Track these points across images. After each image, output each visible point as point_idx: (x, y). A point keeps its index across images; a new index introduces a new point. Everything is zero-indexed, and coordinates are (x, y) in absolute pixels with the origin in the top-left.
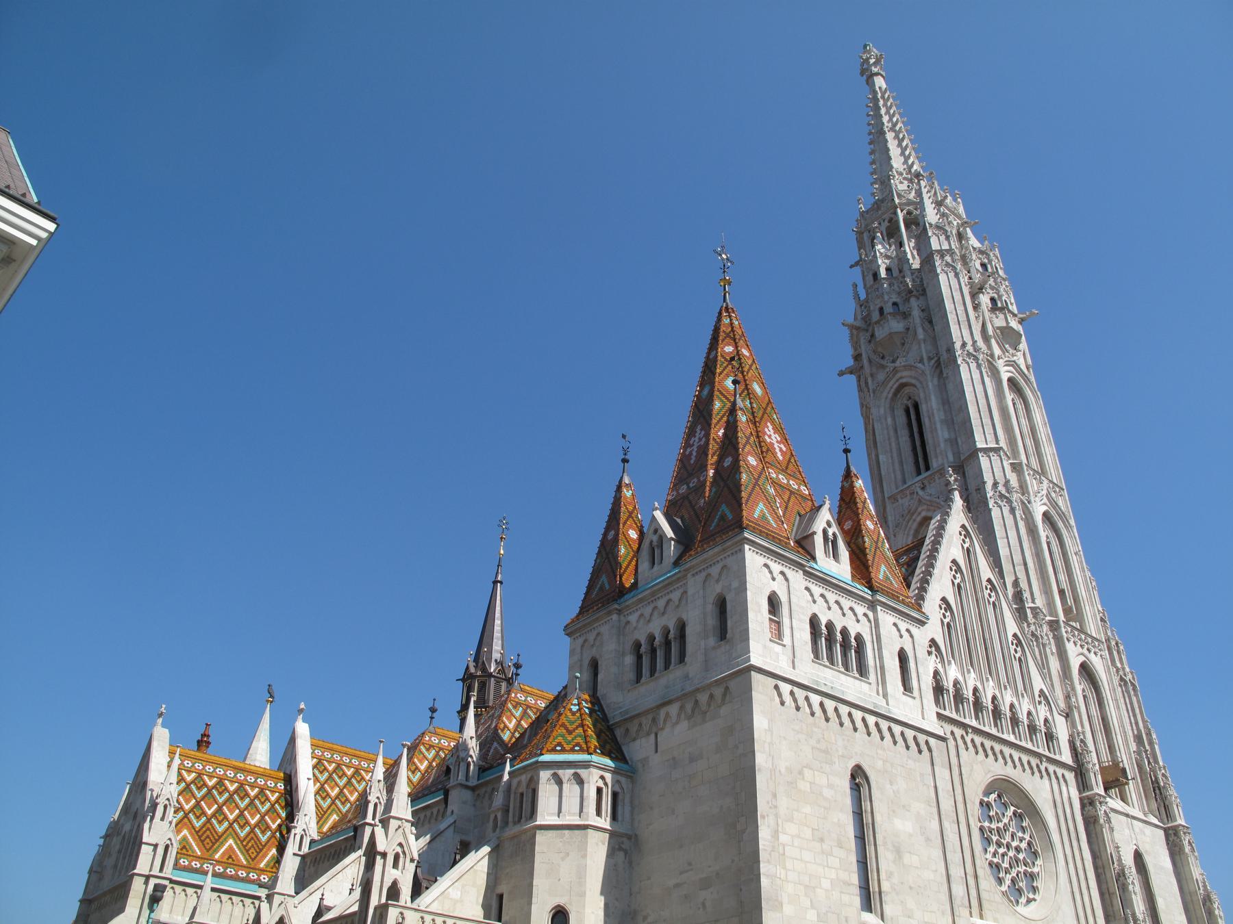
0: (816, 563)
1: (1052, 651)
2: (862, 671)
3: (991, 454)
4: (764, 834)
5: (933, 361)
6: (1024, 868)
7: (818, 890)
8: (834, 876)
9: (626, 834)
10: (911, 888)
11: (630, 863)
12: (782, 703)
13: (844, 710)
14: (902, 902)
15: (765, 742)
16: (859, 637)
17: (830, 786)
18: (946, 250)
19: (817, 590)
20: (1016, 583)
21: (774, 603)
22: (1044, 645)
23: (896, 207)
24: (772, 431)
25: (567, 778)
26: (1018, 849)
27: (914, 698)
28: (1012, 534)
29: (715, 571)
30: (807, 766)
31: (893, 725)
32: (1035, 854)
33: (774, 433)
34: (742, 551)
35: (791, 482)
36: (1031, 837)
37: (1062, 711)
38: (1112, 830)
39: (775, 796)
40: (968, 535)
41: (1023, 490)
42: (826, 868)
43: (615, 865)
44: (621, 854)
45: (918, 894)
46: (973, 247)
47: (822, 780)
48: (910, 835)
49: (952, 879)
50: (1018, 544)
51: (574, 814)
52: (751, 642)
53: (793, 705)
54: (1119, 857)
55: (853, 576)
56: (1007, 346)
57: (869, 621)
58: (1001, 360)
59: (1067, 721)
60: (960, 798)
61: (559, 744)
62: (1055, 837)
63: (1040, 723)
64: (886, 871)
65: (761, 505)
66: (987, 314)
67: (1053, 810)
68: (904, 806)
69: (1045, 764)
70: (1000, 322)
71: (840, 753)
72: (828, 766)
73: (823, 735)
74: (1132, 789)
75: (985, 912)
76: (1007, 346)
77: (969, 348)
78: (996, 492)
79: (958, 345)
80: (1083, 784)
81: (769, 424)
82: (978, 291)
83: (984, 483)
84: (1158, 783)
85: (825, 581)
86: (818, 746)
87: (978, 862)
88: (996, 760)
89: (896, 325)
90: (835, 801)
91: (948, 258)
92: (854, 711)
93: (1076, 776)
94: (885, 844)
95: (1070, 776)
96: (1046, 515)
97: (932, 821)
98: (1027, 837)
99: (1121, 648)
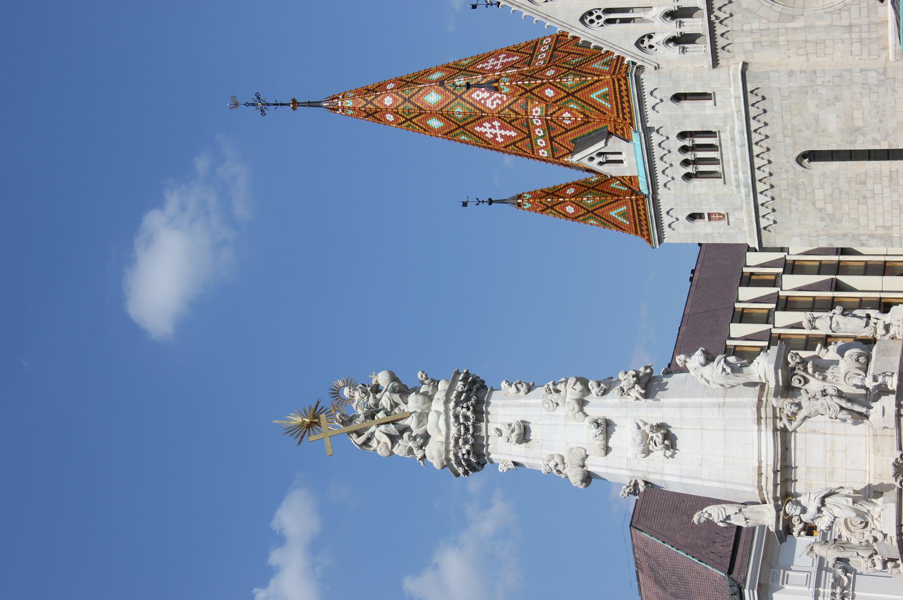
8: (888, 190)
10: (881, 122)
14: (894, 132)
15: (810, 240)
17: (822, 187)
19: (661, 179)
21: (693, 217)
30: (814, 204)
39: (845, 235)
45: (884, 115)
47: (819, 194)
48: (838, 116)
72: (807, 188)
86: (795, 195)
90: (832, 184)
94: (852, 143)
97: (819, 92)
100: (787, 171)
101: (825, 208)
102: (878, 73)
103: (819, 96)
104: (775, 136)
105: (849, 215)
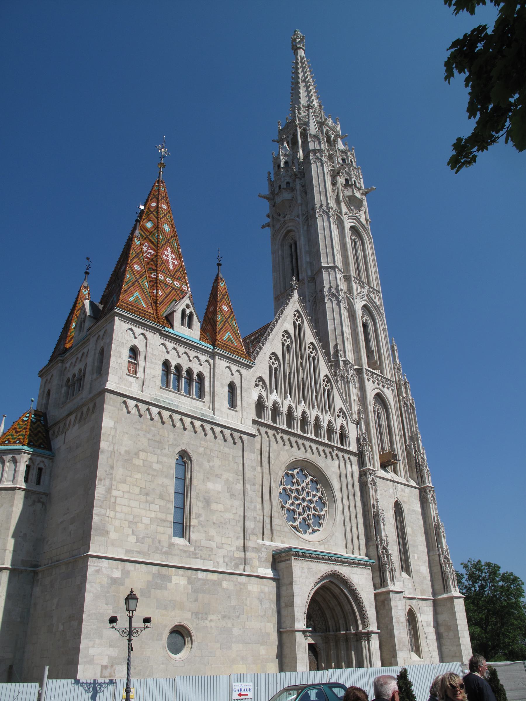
0: (173, 329)
1: (355, 386)
2: (201, 395)
3: (330, 270)
4: (100, 490)
5: (305, 216)
6: (314, 512)
7: (139, 525)
9: (44, 493)
10: (214, 523)
11: (45, 510)
12: (129, 412)
13: (177, 417)
14: (206, 532)
15: (109, 435)
16: (200, 376)
17: (159, 462)
18: (317, 150)
19: (170, 345)
20: (336, 346)
21: (134, 352)
22: (348, 383)
23: (297, 126)
24: (170, 253)
25: (8, 460)
26: (311, 501)
27: (237, 411)
28: (337, 317)
29: (101, 333)
30: (143, 450)
31: (214, 427)
32: (324, 504)
33: (171, 254)
34: (113, 320)
35: (175, 283)
36: (322, 494)
37: (354, 421)
38: (376, 489)
39: (112, 467)
40: (300, 316)
41: (350, 291)
42: (148, 512)
43: (34, 511)
44: (40, 505)
46: (338, 149)
47: (153, 459)
48: (219, 492)
49: (247, 518)
50: (340, 323)
51: (9, 481)
52: (109, 374)
53: (137, 413)
54: (377, 504)
55: (201, 339)
56: (352, 207)
57: (210, 365)
58: (346, 216)
59: (357, 427)
60: (266, 471)
61: (8, 440)
62: (338, 494)
63: (337, 428)
64: (196, 513)
65: (137, 294)
66: (341, 188)
67: (339, 479)
68: (216, 475)
69: (336, 452)
70: (349, 193)
71: (171, 443)
72: (159, 450)
73: (159, 432)
74: (401, 465)
75: (275, 537)
76: (352, 207)
77: (324, 207)
78: (330, 292)
79: (317, 206)
80: (362, 463)
81: (169, 249)
82: (336, 174)
83: (324, 287)
84: (419, 463)
85: (178, 340)
86: (153, 438)
87: (274, 509)
88: (299, 449)
89: (286, 195)
90: (162, 471)
91: (318, 155)
92: (184, 418)
93: (358, 460)
94: (197, 497)
95: (354, 459)
96: (365, 307)
97: (238, 484)
98: (319, 494)
99: (408, 385)
100: (175, 439)
101: (138, 458)
102: (253, 529)
103: (235, 483)
104: (206, 441)
105: (130, 477)
